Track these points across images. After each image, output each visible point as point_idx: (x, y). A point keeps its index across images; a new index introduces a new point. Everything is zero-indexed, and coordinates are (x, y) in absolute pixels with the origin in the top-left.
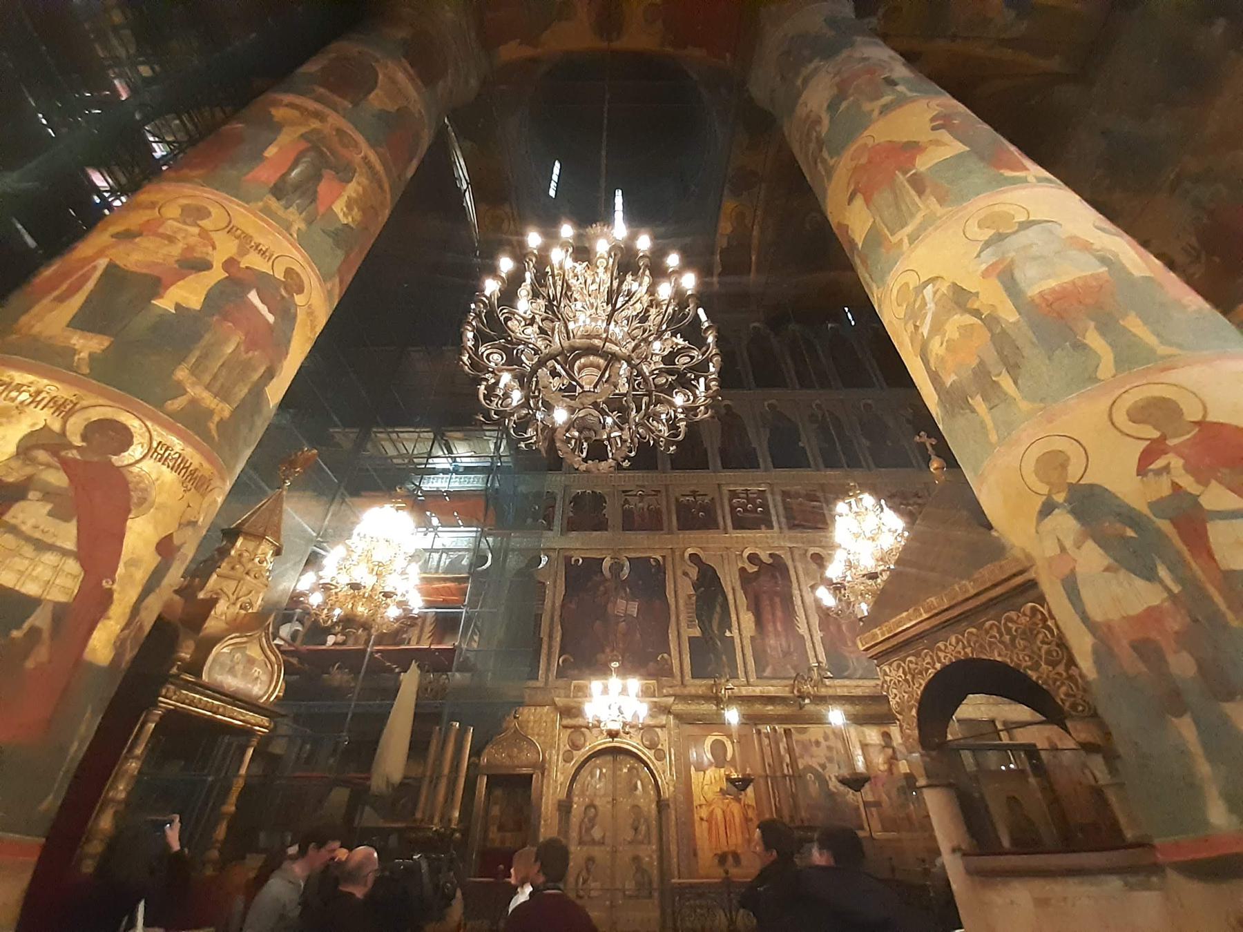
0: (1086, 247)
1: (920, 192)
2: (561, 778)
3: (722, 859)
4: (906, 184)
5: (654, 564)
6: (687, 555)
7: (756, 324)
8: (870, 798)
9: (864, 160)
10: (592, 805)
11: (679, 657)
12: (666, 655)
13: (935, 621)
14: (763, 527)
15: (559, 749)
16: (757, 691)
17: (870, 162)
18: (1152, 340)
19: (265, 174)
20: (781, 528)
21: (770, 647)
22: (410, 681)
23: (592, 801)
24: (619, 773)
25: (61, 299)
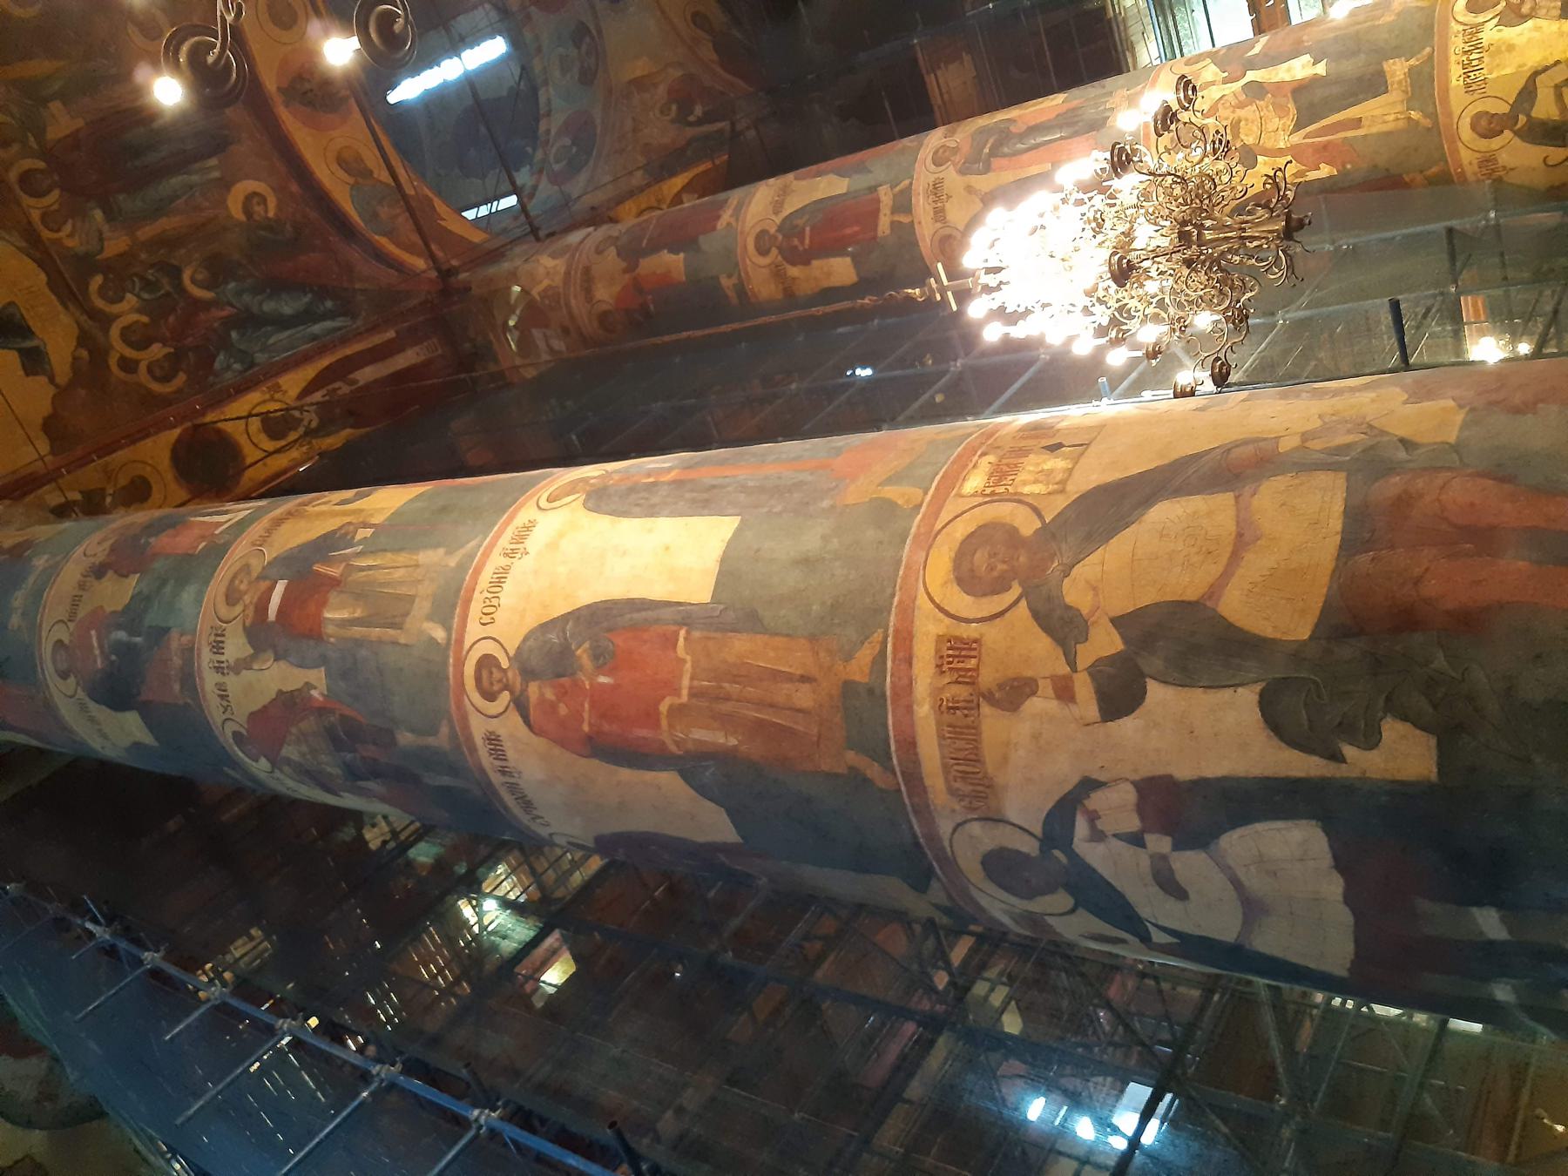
25: (1357, 123)
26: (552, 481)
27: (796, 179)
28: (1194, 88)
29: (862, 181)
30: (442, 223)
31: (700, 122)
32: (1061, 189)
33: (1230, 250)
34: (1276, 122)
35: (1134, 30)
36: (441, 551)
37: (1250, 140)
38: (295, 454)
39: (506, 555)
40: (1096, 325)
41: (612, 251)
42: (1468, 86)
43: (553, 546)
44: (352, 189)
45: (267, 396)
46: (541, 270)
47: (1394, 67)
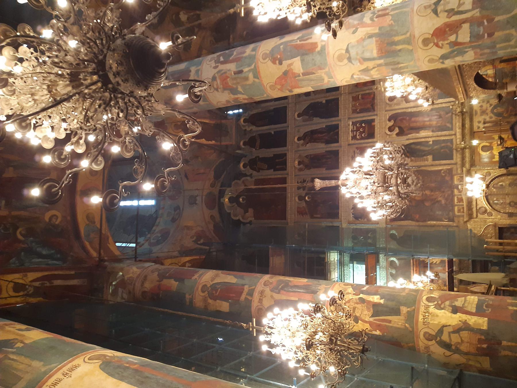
0: (363, 39)
1: (314, 73)
2: (499, 217)
11: (442, 166)
12: (442, 171)
13: (461, 83)
14: (373, 124)
15: (487, 219)
16: (459, 131)
20: (374, 115)
23: (508, 204)
25: (390, 322)
26: (94, 352)
27: (222, 273)
28: (344, 295)
29: (241, 282)
30: (108, 245)
31: (201, 244)
32: (298, 311)
33: (344, 350)
34: (366, 312)
35: (332, 267)
36: (42, 363)
37: (358, 315)
38: (18, 299)
39: (63, 374)
40: (298, 359)
41: (157, 273)
42: (424, 322)
43: (81, 378)
44: (86, 225)
45: (21, 277)
46: (131, 271)
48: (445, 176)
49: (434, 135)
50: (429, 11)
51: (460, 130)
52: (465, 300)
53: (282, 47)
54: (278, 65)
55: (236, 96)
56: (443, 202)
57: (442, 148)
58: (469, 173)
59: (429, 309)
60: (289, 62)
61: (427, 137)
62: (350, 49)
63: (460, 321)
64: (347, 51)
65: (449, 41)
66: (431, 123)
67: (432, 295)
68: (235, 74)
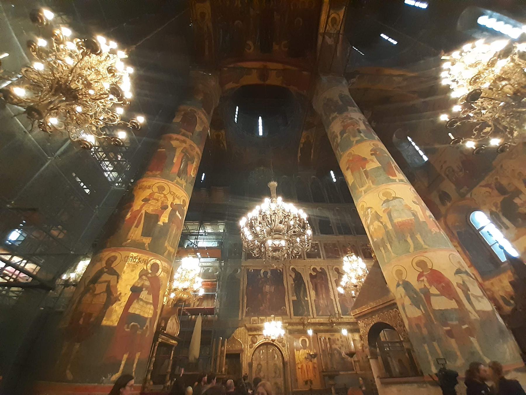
0: (409, 209)
1: (367, 178)
2: (249, 355)
3: (306, 382)
4: (363, 173)
5: (279, 271)
6: (291, 268)
7: (314, 177)
8: (356, 359)
9: (351, 158)
10: (259, 364)
11: (289, 308)
14: (317, 257)
15: (248, 344)
16: (317, 320)
17: (352, 160)
18: (423, 243)
19: (175, 169)
21: (321, 303)
22: (199, 320)
24: (269, 352)
25: (137, 226)
34: (151, 208)
47: (148, 239)
48: (281, 310)
49: (312, 302)
50: (458, 266)
51: (318, 322)
52: (147, 303)
53: (386, 155)
54: (370, 153)
55: (339, 135)
56: (261, 308)
57: (303, 307)
58: (285, 328)
59: (143, 264)
60: (375, 160)
61: (310, 296)
62: (397, 199)
63: (120, 294)
64: (395, 198)
65: (429, 287)
66: (321, 299)
67: (160, 270)
68: (357, 129)
